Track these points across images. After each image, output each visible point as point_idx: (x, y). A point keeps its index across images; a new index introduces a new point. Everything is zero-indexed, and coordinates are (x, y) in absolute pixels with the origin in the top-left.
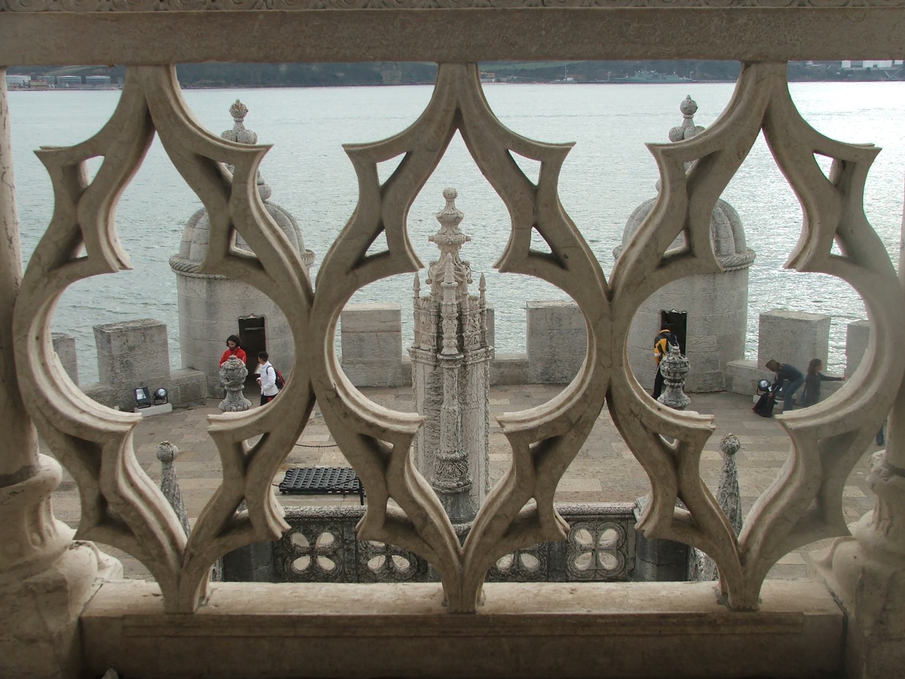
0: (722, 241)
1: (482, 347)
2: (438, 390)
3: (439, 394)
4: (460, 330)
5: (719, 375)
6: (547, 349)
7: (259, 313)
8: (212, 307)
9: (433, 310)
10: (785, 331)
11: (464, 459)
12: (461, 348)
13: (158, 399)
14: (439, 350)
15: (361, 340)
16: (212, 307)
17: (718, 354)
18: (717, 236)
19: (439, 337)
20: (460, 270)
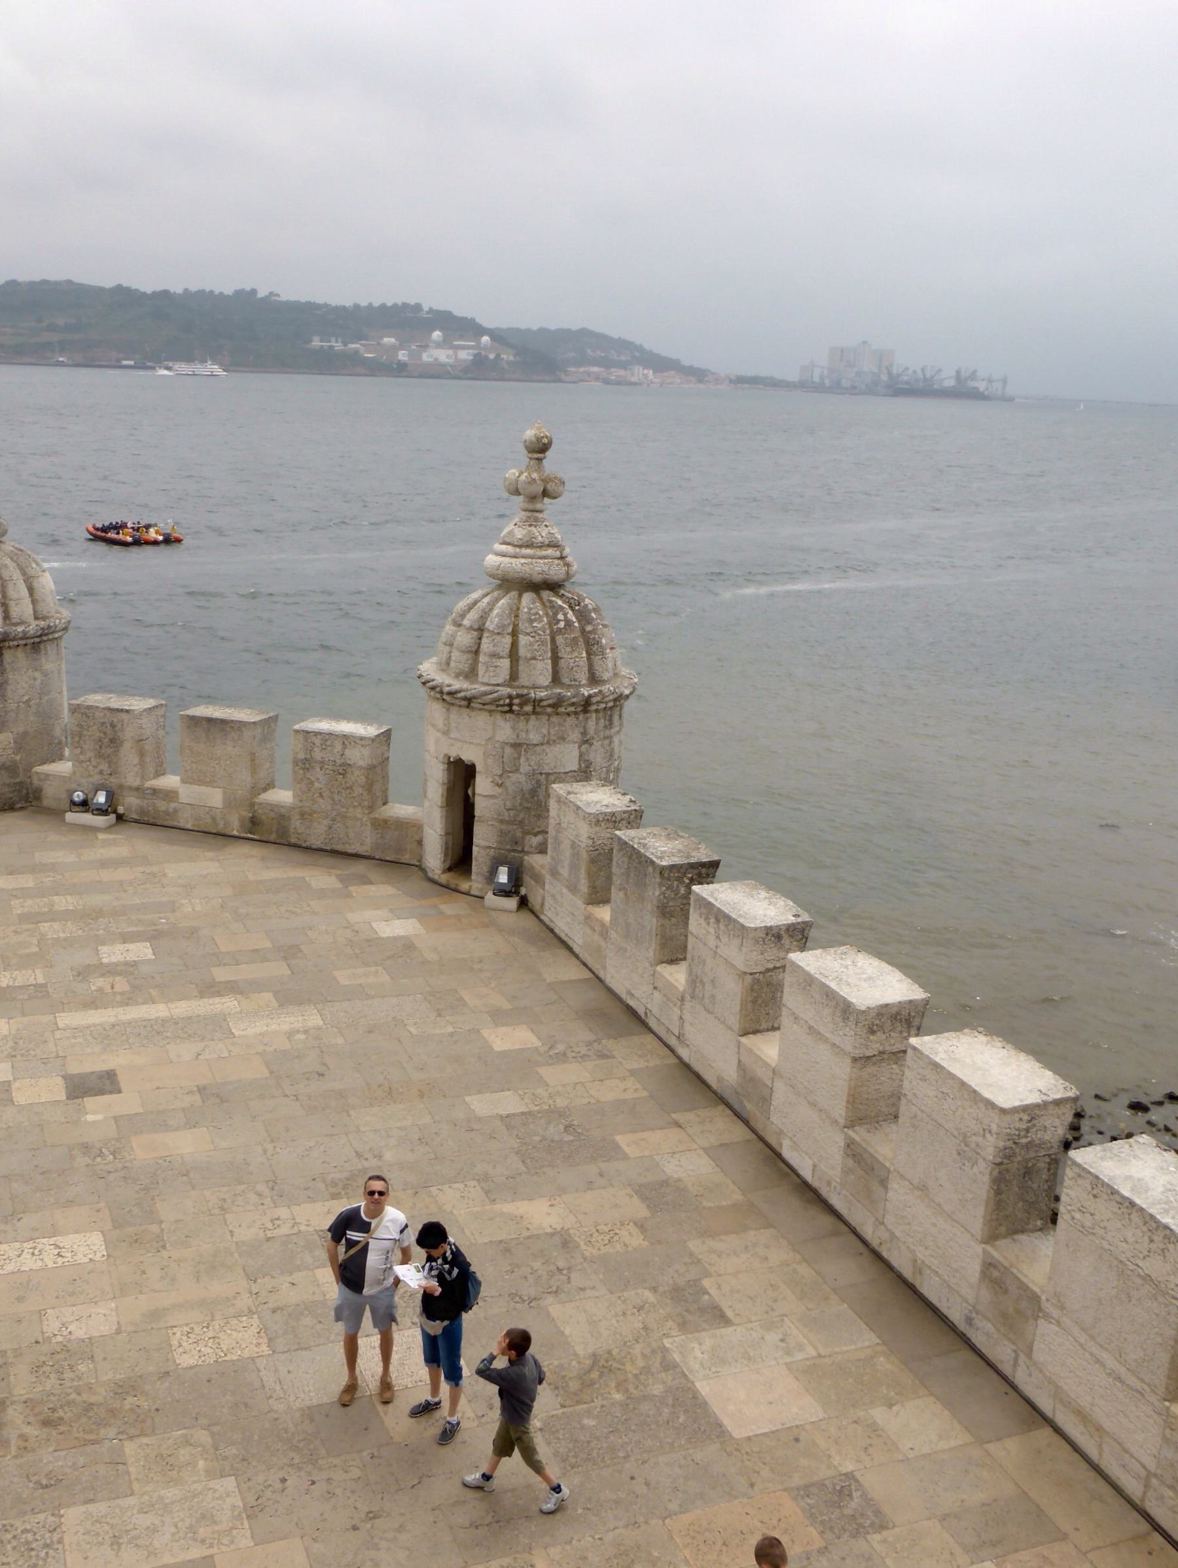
0: (12, 604)
10: (103, 723)
17: (18, 758)
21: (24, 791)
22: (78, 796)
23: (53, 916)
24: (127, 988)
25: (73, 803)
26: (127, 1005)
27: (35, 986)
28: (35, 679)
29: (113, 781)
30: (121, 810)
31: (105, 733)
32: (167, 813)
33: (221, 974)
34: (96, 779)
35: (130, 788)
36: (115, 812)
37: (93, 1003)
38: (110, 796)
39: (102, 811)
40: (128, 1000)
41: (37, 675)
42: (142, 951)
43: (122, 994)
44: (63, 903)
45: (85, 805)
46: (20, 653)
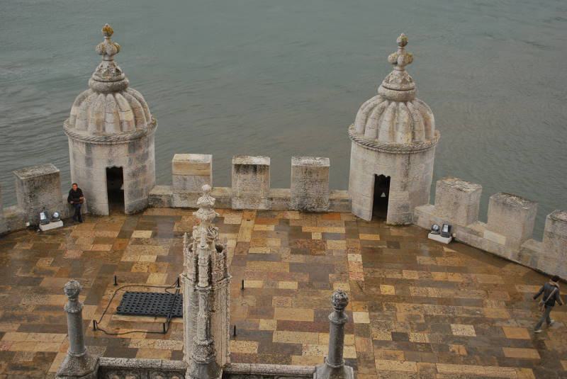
1: (225, 278)
2: (197, 303)
3: (197, 305)
4: (210, 270)
5: (409, 214)
6: (302, 190)
7: (118, 165)
8: (89, 161)
9: (194, 259)
10: (452, 195)
11: (211, 344)
12: (210, 282)
13: (54, 220)
14: (197, 281)
15: (185, 180)
16: (89, 161)
17: (410, 202)
19: (197, 274)
20: (209, 235)
22: (436, 227)
23: (429, 300)
24: (465, 353)
25: (433, 229)
26: (466, 364)
27: (425, 344)
28: (422, 167)
29: (452, 222)
30: (454, 235)
33: (509, 352)
34: (446, 219)
36: (452, 235)
37: (452, 360)
38: (450, 228)
39: (445, 235)
40: (467, 360)
41: (423, 165)
42: (469, 331)
43: (464, 356)
44: (433, 292)
45: (438, 232)
46: (417, 156)
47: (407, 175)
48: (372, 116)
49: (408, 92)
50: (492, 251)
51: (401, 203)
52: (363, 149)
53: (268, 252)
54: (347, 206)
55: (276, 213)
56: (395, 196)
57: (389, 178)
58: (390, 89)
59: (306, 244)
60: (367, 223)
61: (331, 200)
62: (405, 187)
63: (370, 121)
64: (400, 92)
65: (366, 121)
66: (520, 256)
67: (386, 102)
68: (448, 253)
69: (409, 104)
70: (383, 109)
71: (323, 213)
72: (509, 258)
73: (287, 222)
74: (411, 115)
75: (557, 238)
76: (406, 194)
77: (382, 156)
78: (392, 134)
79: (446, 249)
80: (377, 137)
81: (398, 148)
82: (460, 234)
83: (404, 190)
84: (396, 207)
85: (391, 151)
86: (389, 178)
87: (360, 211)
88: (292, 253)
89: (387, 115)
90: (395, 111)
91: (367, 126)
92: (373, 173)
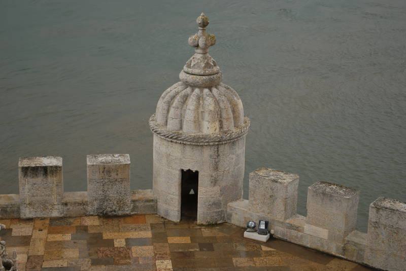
6: (100, 192)
10: (267, 187)
17: (221, 199)
18: (221, 117)
21: (223, 215)
22: (251, 224)
25: (248, 227)
28: (232, 159)
29: (269, 217)
30: (272, 232)
31: (267, 192)
32: (297, 237)
34: (261, 214)
35: (279, 222)
36: (269, 232)
38: (267, 224)
39: (262, 232)
41: (234, 156)
45: (254, 229)
46: (227, 147)
47: (216, 168)
48: (174, 105)
49: (212, 77)
50: (314, 246)
51: (212, 200)
52: (165, 142)
53: (65, 265)
54: (152, 207)
55: (71, 220)
56: (205, 192)
57: (197, 172)
58: (192, 74)
59: (108, 252)
60: (175, 224)
61: (134, 201)
62: (215, 182)
63: (172, 111)
64: (204, 77)
65: (168, 111)
66: (344, 249)
67: (189, 90)
68: (267, 252)
69: (214, 90)
70: (186, 98)
71: (125, 216)
72: (333, 253)
73: (85, 229)
74: (217, 102)
75: (383, 228)
76: (217, 189)
77: (188, 149)
78: (198, 123)
79: (264, 248)
80: (181, 128)
81: (205, 139)
82: (278, 230)
83: (215, 185)
84: (207, 204)
85: (198, 143)
86: (197, 172)
87: (167, 212)
88: (92, 264)
89: (191, 104)
90: (199, 98)
91: (170, 115)
92: (179, 169)
